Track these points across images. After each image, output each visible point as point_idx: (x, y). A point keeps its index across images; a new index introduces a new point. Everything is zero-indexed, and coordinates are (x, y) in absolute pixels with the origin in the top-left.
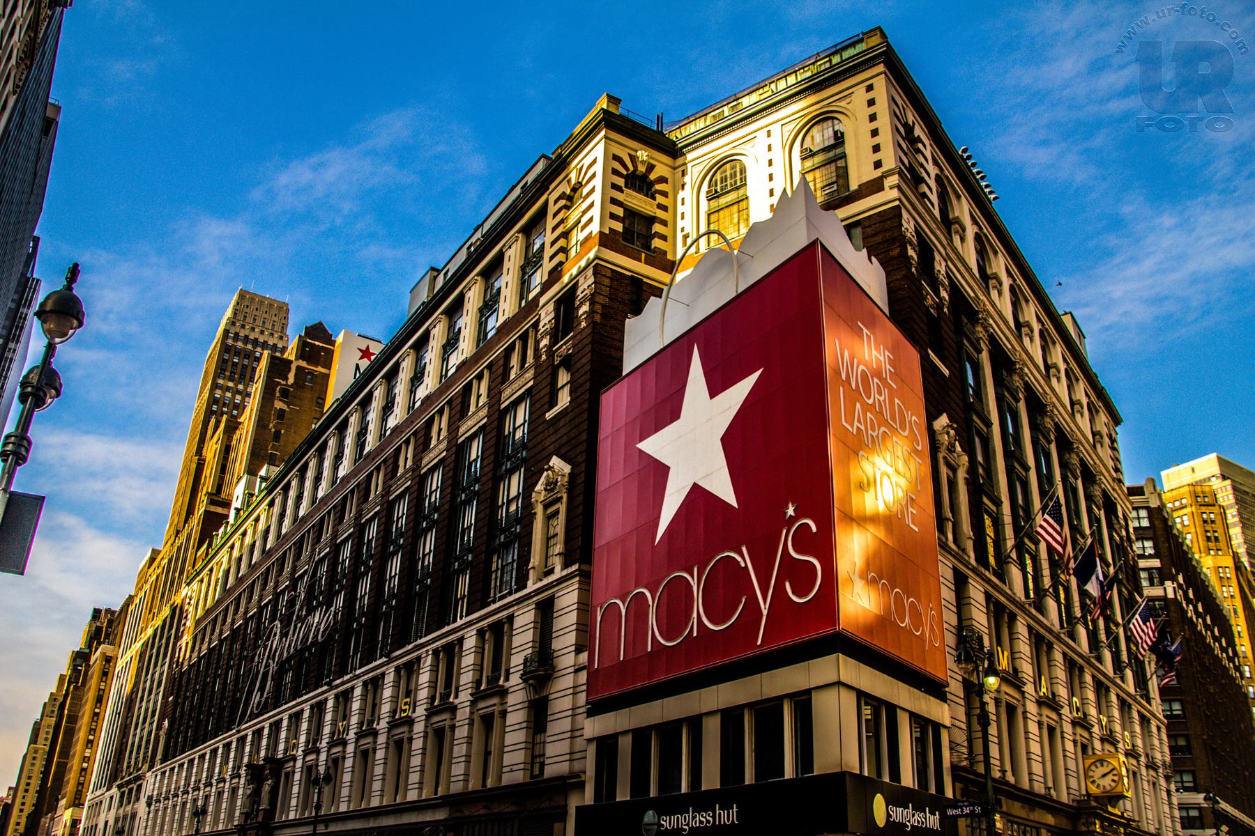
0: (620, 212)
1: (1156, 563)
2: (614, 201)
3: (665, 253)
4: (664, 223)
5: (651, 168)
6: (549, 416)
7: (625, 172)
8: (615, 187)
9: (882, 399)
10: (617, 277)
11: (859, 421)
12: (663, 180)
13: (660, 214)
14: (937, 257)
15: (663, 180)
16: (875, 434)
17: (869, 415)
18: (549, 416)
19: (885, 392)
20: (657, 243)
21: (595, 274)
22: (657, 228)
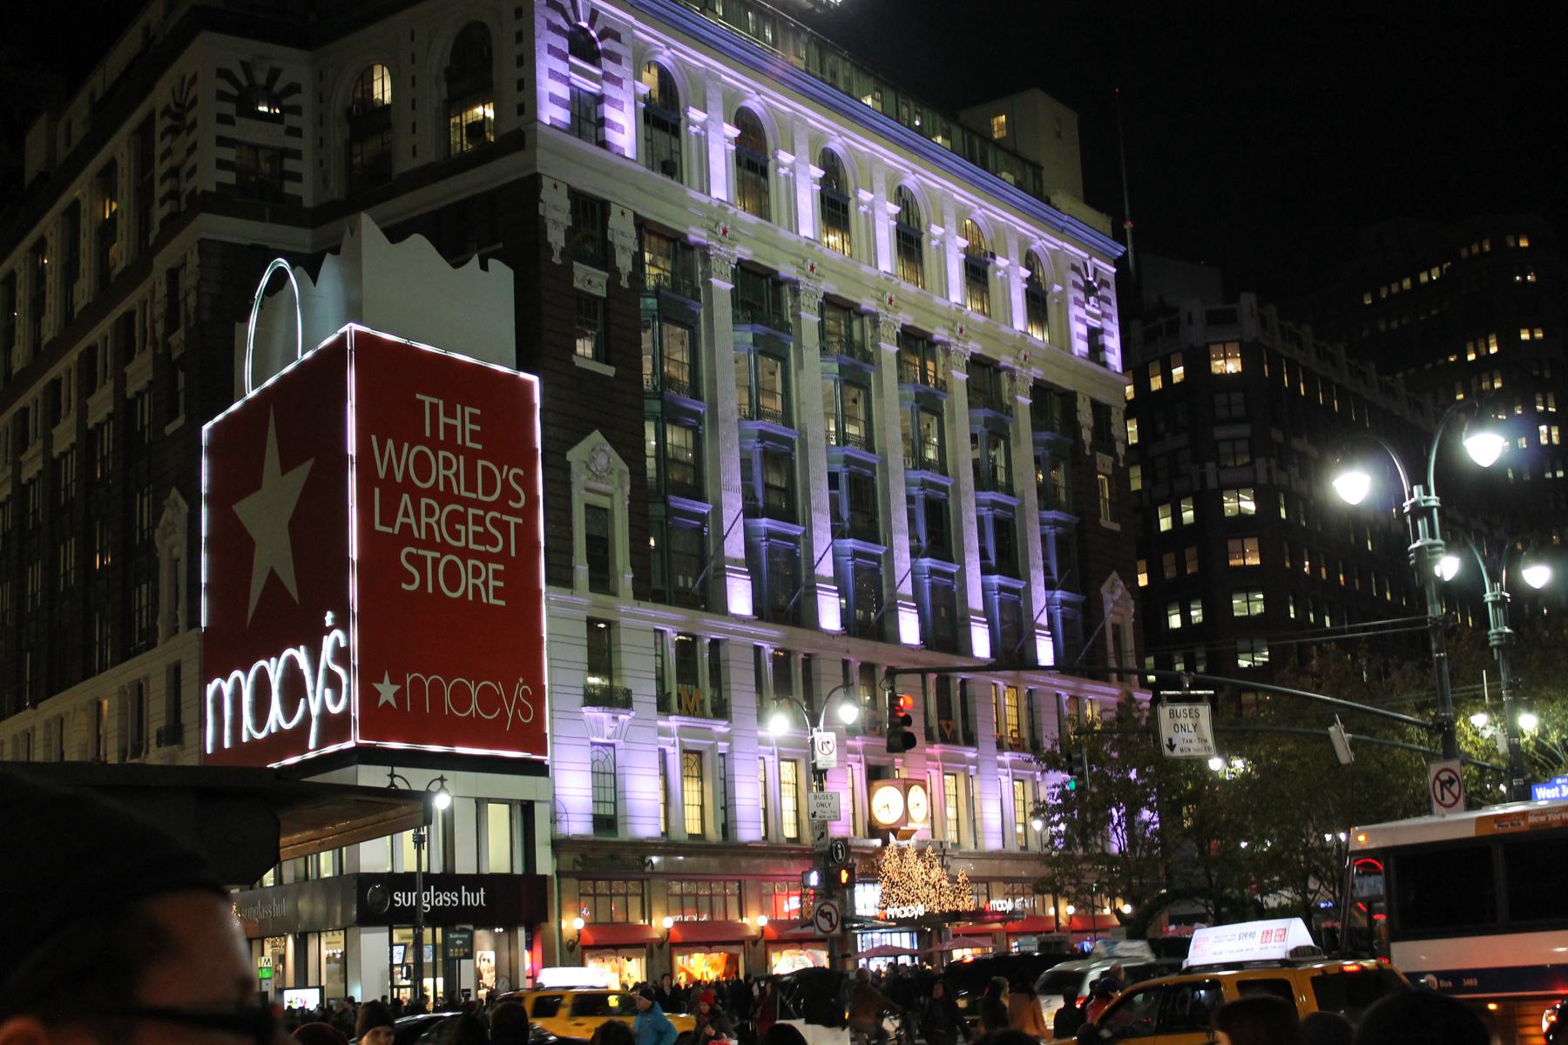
0: (230, 154)
1: (1245, 430)
2: (222, 141)
3: (300, 199)
4: (297, 155)
5: (274, 74)
6: (170, 429)
7: (235, 92)
8: (224, 119)
9: (450, 473)
10: (229, 249)
11: (406, 514)
12: (294, 89)
13: (291, 143)
14: (615, 210)
15: (294, 89)
16: (432, 521)
17: (424, 501)
18: (170, 429)
19: (460, 463)
20: (290, 188)
21: (201, 252)
22: (290, 164)
